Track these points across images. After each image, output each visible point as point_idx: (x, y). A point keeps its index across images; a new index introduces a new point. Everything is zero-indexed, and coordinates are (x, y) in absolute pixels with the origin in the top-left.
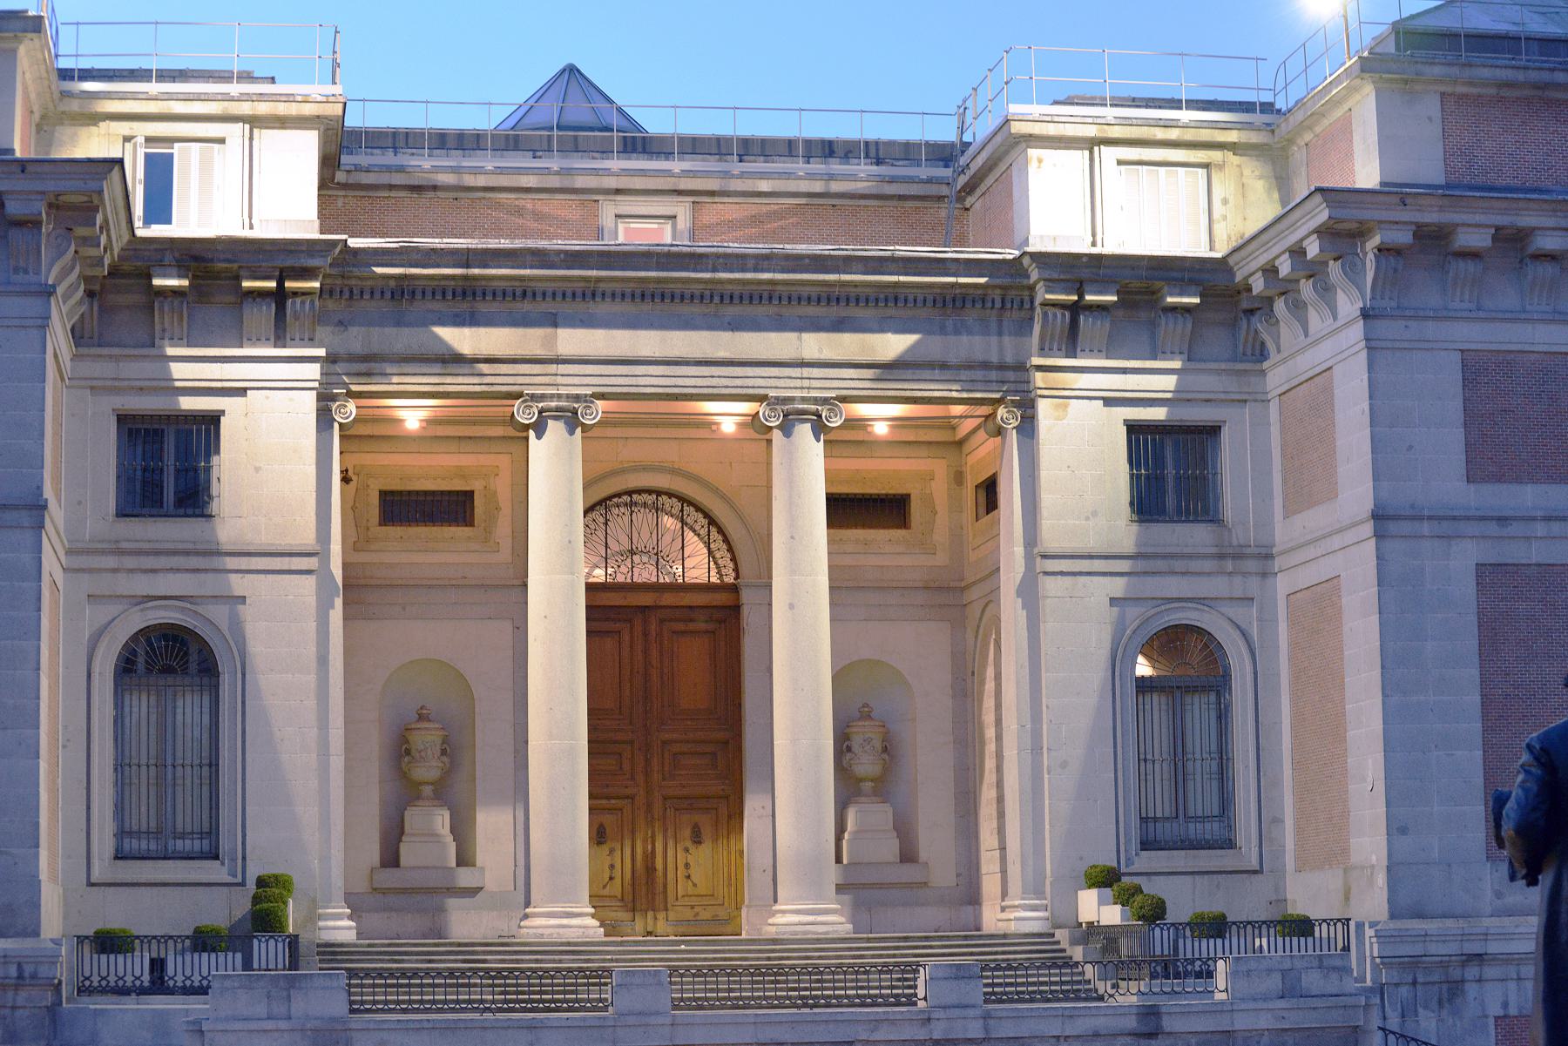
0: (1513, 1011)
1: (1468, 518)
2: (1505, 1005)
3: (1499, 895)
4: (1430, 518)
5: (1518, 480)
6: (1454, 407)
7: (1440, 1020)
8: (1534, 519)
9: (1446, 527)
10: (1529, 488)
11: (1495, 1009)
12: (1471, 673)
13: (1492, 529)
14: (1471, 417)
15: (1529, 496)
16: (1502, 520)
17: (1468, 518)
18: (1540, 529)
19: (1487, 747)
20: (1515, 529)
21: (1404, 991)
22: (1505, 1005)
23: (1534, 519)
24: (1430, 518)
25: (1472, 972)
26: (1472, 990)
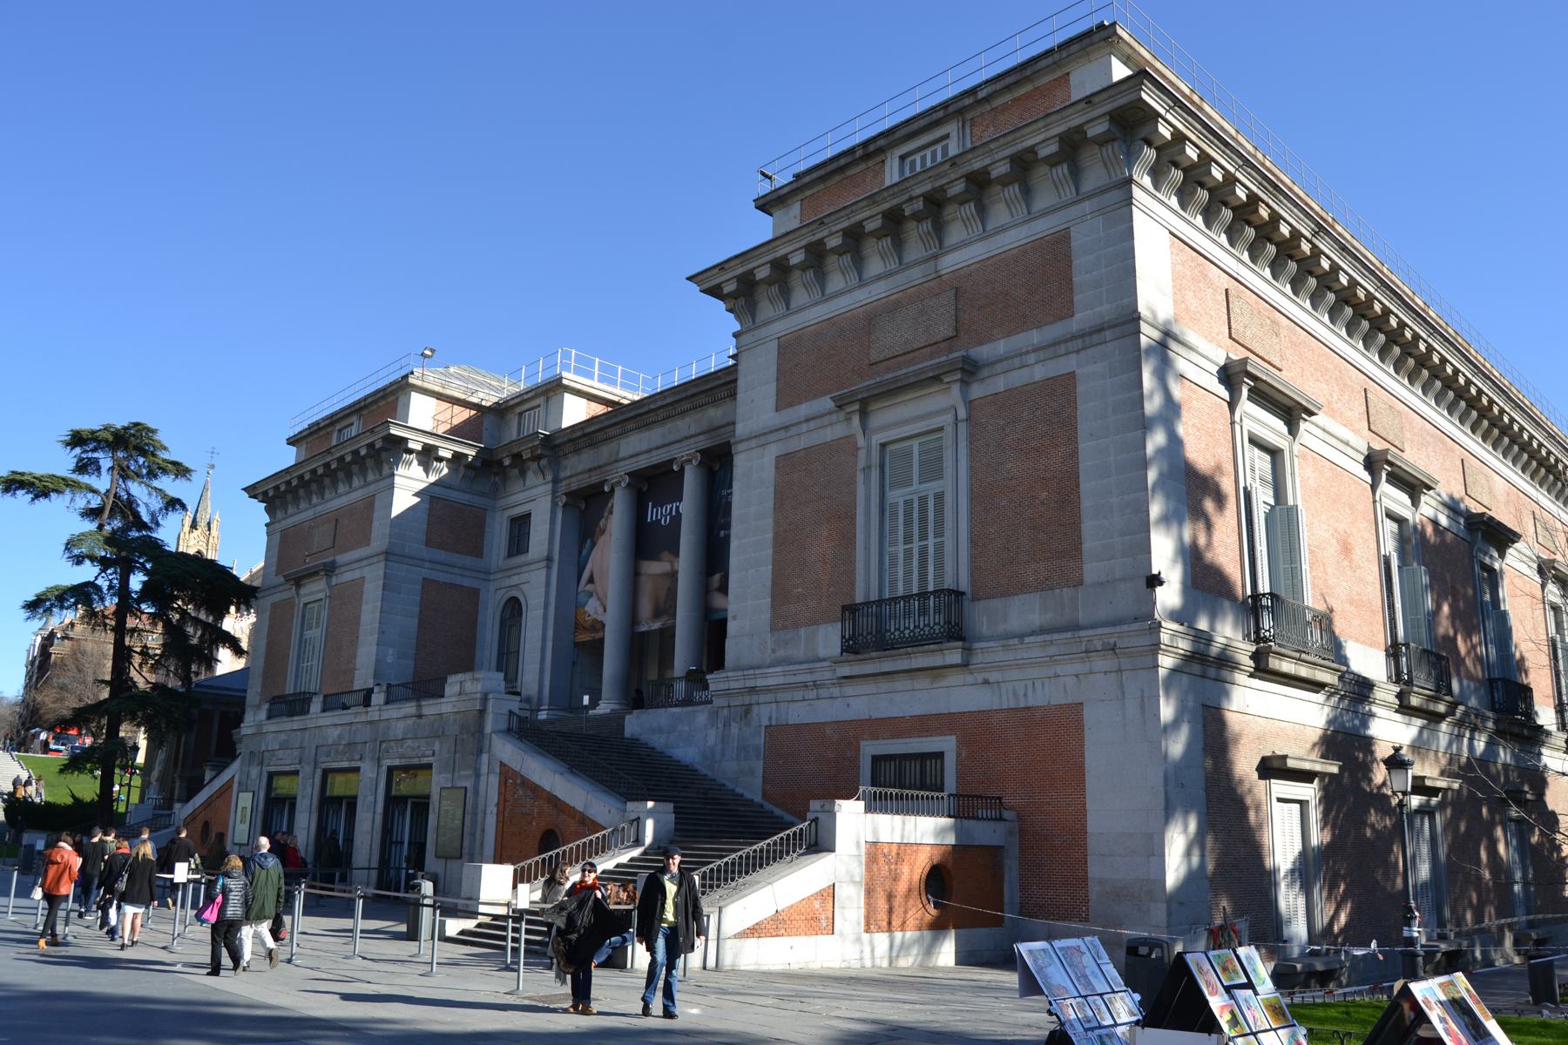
0: (774, 723)
1: (771, 432)
2: (770, 718)
3: (774, 651)
4: (755, 437)
5: (800, 403)
6: (772, 371)
7: (740, 729)
8: (800, 423)
9: (762, 440)
10: (803, 406)
11: (765, 722)
12: (769, 522)
13: (782, 434)
14: (781, 373)
15: (804, 410)
16: (786, 428)
17: (771, 432)
18: (804, 427)
19: (776, 564)
20: (793, 431)
21: (726, 711)
22: (770, 718)
23: (800, 423)
24: (755, 437)
25: (754, 698)
26: (755, 709)
